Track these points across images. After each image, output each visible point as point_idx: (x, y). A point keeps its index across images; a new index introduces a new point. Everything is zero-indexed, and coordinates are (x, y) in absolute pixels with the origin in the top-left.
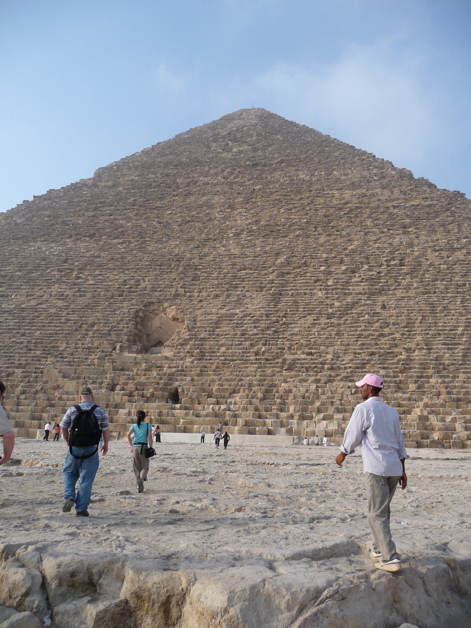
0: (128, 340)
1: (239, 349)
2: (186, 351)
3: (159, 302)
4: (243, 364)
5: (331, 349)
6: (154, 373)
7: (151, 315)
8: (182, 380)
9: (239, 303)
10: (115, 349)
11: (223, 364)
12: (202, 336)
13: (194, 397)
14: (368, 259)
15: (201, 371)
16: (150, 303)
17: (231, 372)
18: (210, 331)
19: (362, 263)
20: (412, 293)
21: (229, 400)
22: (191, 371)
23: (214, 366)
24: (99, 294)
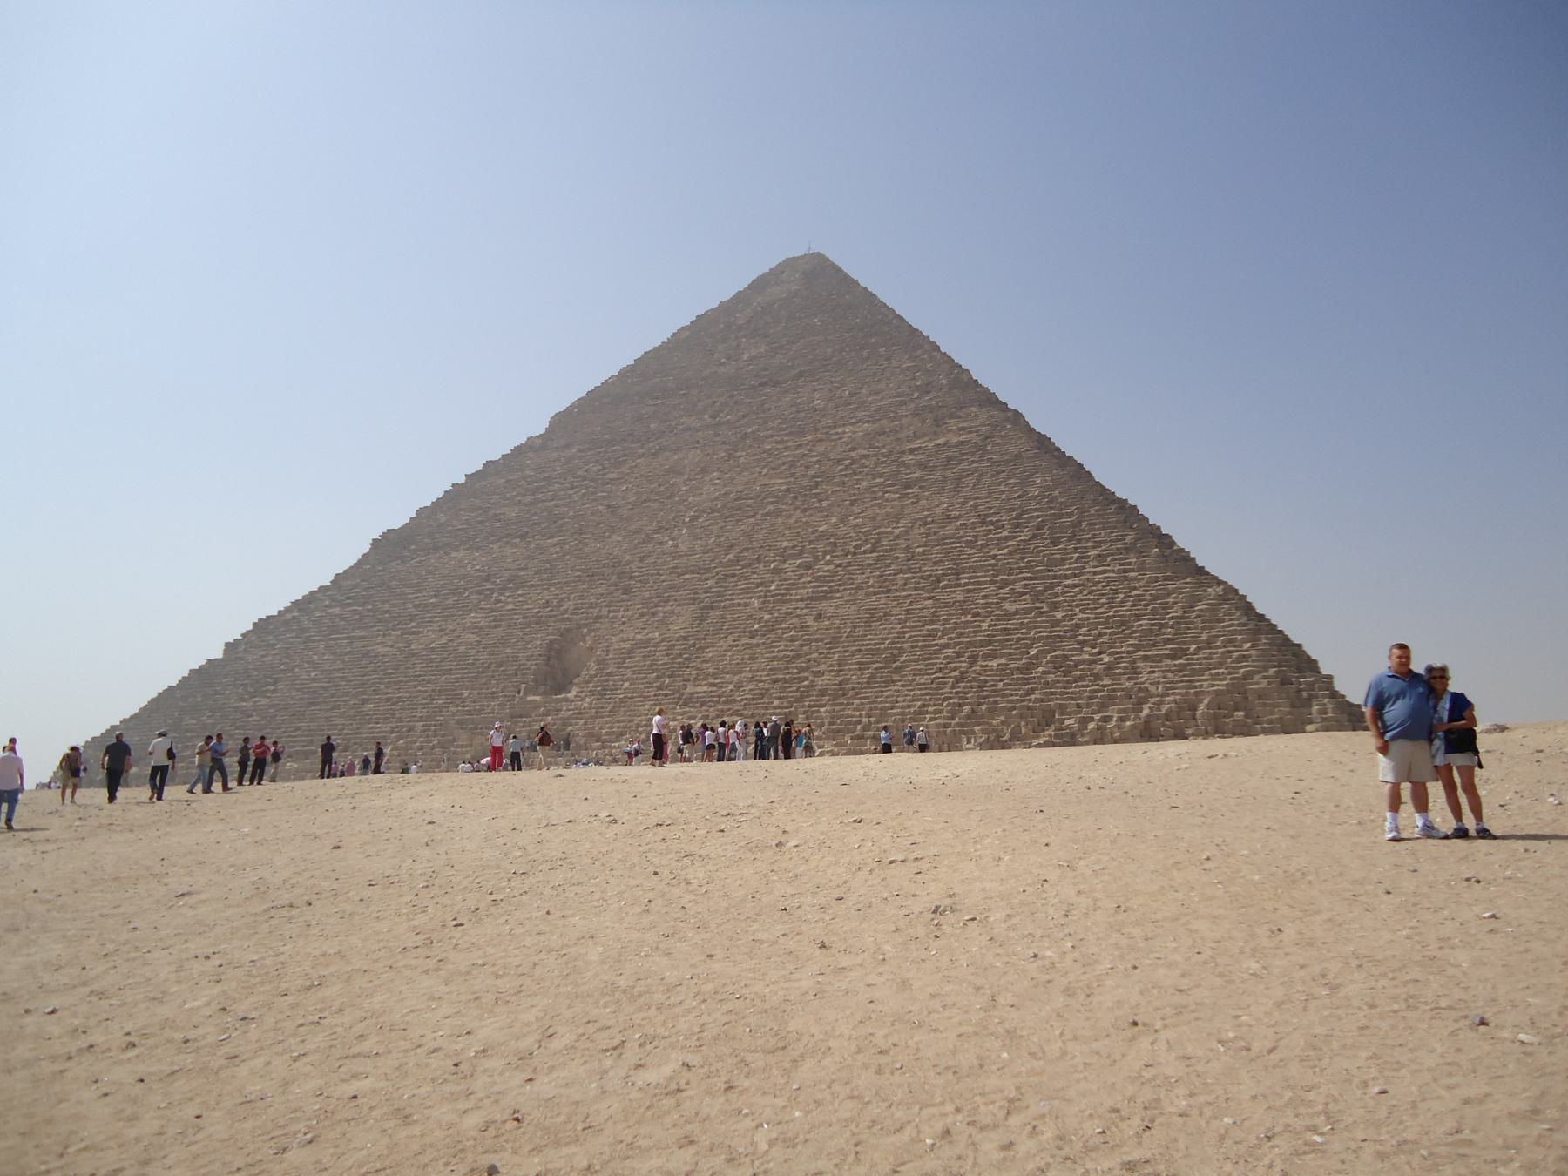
0: (535, 681)
5: (735, 679)
9: (663, 622)
14: (835, 544)
16: (568, 630)
19: (825, 553)
20: (861, 595)
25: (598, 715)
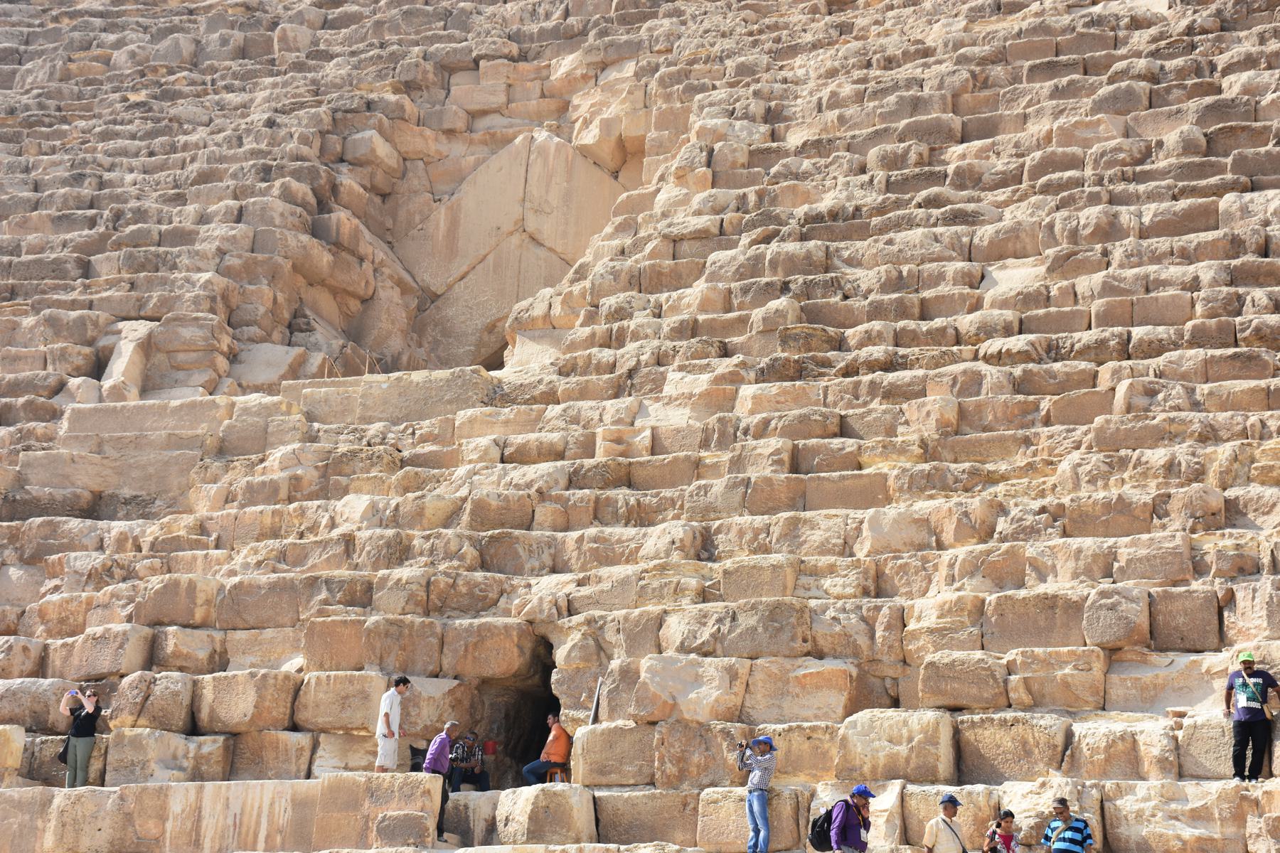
1: (1187, 257)
2: (669, 322)
3: (523, 57)
4: (1248, 365)
6: (352, 508)
7: (457, 149)
8: (606, 555)
10: (97, 368)
11: (1019, 386)
12: (826, 203)
13: (707, 693)
15: (796, 463)
17: (1105, 442)
18: (892, 162)
21: (1094, 731)
22: (697, 468)
23: (923, 419)
24: (107, 61)
25: (806, 475)
